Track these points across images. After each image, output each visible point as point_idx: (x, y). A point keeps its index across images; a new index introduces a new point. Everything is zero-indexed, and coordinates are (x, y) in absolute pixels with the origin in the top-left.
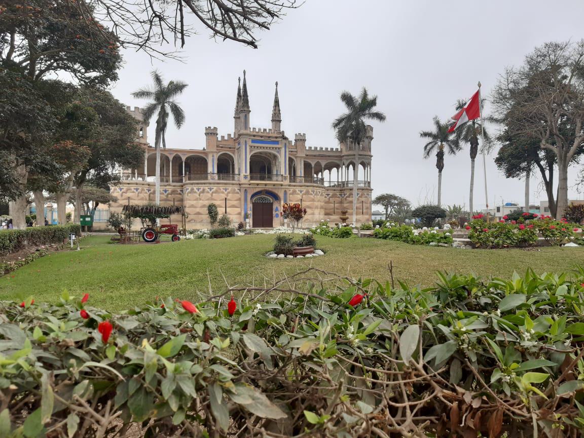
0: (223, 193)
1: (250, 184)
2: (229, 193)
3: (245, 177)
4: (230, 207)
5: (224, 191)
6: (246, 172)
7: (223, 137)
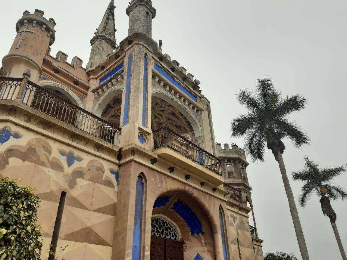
0: (57, 166)
1: (154, 161)
2: (79, 174)
3: (143, 134)
4: (72, 237)
5: (63, 160)
6: (145, 123)
7: (62, 56)
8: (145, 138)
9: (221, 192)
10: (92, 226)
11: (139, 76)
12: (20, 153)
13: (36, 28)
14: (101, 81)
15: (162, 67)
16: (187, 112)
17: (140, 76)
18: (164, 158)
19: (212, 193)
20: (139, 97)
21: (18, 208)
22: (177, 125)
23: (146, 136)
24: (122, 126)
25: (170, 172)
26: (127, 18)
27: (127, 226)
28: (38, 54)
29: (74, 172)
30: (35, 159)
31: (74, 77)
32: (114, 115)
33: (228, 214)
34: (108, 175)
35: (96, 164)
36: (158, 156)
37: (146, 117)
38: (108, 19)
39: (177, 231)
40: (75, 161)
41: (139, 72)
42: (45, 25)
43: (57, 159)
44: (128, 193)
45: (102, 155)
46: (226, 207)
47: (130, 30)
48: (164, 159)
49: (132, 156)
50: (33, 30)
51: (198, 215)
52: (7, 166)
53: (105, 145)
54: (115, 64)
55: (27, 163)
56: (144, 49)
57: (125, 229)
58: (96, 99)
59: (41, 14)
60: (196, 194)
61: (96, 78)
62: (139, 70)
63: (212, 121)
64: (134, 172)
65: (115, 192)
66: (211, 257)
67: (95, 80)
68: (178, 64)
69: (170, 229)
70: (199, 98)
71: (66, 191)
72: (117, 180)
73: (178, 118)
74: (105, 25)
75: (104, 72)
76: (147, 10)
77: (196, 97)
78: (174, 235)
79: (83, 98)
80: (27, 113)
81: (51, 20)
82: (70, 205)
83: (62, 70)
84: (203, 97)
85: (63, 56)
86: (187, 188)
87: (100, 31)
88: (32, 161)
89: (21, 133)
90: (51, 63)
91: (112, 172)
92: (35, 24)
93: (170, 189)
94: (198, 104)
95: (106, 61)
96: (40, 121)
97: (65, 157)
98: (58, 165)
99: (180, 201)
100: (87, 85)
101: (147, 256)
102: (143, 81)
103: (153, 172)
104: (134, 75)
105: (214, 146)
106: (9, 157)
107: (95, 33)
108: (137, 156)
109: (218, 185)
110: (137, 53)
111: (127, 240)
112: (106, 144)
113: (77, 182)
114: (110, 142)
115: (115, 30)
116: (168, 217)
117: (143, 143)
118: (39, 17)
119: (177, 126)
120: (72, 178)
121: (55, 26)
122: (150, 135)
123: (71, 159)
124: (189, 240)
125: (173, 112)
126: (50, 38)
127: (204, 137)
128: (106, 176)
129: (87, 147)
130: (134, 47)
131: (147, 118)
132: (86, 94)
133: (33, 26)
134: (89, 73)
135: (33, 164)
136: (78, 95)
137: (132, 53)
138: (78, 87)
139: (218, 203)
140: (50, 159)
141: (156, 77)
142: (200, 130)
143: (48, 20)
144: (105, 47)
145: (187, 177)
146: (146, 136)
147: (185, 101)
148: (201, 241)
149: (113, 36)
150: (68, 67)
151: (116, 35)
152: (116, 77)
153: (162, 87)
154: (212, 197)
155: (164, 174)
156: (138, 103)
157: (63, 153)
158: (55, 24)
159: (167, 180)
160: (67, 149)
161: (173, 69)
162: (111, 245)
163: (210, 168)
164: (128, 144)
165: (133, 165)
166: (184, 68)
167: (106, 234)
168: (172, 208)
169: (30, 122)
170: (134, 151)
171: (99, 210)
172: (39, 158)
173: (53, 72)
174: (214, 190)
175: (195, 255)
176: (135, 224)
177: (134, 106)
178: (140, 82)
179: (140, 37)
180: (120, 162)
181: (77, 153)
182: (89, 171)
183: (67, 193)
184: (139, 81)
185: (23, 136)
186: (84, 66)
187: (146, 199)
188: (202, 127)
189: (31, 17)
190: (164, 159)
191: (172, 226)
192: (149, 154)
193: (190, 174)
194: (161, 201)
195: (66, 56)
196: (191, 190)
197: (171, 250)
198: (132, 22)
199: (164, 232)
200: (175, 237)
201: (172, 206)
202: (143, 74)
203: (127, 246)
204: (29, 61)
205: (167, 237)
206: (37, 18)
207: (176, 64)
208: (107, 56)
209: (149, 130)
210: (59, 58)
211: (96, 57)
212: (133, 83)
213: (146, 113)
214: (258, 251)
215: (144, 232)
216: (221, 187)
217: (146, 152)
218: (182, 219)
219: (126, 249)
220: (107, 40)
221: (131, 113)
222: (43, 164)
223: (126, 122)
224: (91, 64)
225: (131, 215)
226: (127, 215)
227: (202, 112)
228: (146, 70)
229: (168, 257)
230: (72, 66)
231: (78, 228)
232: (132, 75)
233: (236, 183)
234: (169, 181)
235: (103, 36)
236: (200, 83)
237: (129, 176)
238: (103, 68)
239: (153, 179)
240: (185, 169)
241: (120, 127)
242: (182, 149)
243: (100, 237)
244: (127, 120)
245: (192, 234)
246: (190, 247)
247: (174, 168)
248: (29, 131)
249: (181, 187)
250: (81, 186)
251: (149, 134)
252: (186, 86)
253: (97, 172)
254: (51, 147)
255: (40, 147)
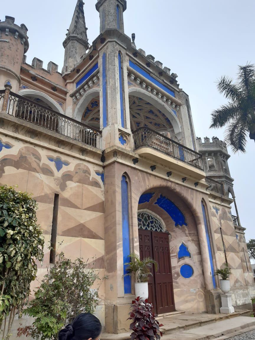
0: (47, 171)
1: (135, 161)
2: (68, 177)
3: (123, 135)
4: (68, 233)
5: (52, 166)
6: (124, 124)
7: (38, 62)
8: (126, 139)
9: (203, 186)
10: (85, 223)
11: (115, 75)
12: (14, 162)
13: (9, 37)
14: (77, 84)
15: (137, 63)
16: (165, 108)
17: (116, 75)
18: (146, 157)
19: (194, 187)
20: (116, 97)
21: (19, 211)
22: (155, 123)
23: (126, 137)
24: (103, 129)
25: (152, 170)
26: (98, 14)
27: (116, 221)
28: (15, 63)
29: (63, 176)
30: (28, 166)
31: (52, 83)
32: (93, 118)
33: (211, 206)
34: (94, 176)
35: (82, 167)
36: (140, 155)
37: (125, 118)
38: (78, 17)
39: (162, 223)
40: (63, 165)
41: (115, 72)
42: (18, 32)
43: (47, 165)
44: (114, 192)
45: (87, 158)
46: (208, 199)
47: (102, 27)
48: (145, 158)
49: (114, 158)
50: (7, 39)
51: (181, 208)
52: (3, 174)
53: (89, 149)
54: (90, 65)
55: (20, 170)
56: (118, 46)
57: (114, 224)
58: (75, 103)
59: (12, 21)
60: (178, 189)
61: (73, 82)
62: (114, 69)
63: (191, 116)
64: (118, 173)
65: (102, 191)
66: (196, 246)
67: (72, 84)
68: (153, 58)
69: (155, 222)
70: (178, 93)
71: (58, 193)
72: (103, 181)
73: (156, 115)
74: (76, 24)
75: (80, 75)
76: (117, 3)
77: (174, 92)
78: (159, 227)
79: (62, 103)
80: (14, 123)
81: (23, 26)
82: (64, 205)
83: (39, 77)
84: (181, 91)
85: (38, 62)
86: (169, 184)
87: (71, 31)
88: (25, 168)
89: (11, 143)
90: (28, 71)
91: (98, 173)
92: (7, 32)
93: (153, 186)
94: (177, 99)
95: (81, 63)
96: (27, 131)
97: (54, 162)
98: (48, 170)
99: (163, 196)
100: (65, 90)
101: (136, 246)
102: (118, 81)
103: (135, 171)
104: (109, 75)
105: (194, 141)
106: (5, 166)
107: (67, 35)
108: (119, 157)
109: (200, 180)
110: (111, 51)
111: (117, 233)
112: (89, 148)
113: (67, 185)
114: (93, 146)
115: (86, 29)
116: (153, 211)
117: (123, 144)
118: (11, 24)
119: (156, 124)
120: (62, 181)
121: (28, 32)
122: (130, 136)
123: (59, 164)
124: (174, 231)
125: (151, 110)
126: (24, 45)
127: (184, 133)
128: (93, 178)
129: (72, 152)
130: (107, 45)
131: (126, 118)
132: (65, 100)
133: (7, 35)
134: (65, 78)
135: (26, 171)
136: (57, 101)
137: (106, 52)
138: (56, 93)
139: (200, 197)
140: (41, 165)
141: (132, 75)
142: (180, 126)
143: (20, 26)
144: (78, 48)
145: (169, 174)
146: (126, 137)
147: (162, 97)
148: (185, 232)
149: (85, 36)
150: (45, 74)
151: (87, 33)
152: (91, 79)
153: (138, 85)
154: (194, 191)
155: (147, 173)
156: (116, 105)
157: (51, 159)
158: (27, 30)
159: (149, 177)
160: (55, 155)
161: (148, 64)
162: (103, 238)
163: (191, 163)
164: (110, 146)
165: (116, 165)
166: (160, 62)
167: (98, 229)
168: (156, 203)
169: (18, 132)
170: (116, 153)
171: (88, 209)
172: (31, 165)
173: (31, 81)
174: (196, 184)
175: (180, 244)
176: (123, 218)
177: (112, 108)
178: (116, 82)
179: (112, 33)
180: (104, 164)
181: (64, 158)
182: (77, 174)
183: (59, 195)
184: (115, 81)
185: (14, 146)
186: (60, 70)
187: (131, 196)
188: (181, 122)
189: (3, 25)
190: (145, 158)
191: (157, 219)
192: (131, 154)
193: (171, 170)
194: (145, 198)
195: (41, 62)
196: (173, 186)
197: (157, 241)
198: (103, 18)
199: (150, 225)
200: (160, 229)
201: (156, 201)
202: (118, 73)
203: (117, 238)
204: (8, 71)
205: (153, 229)
206: (9, 26)
207: (151, 58)
208: (81, 58)
209: (128, 130)
210: (35, 65)
211: (70, 60)
212: (109, 84)
213: (124, 114)
214: (241, 238)
215: (132, 226)
216: (203, 181)
217: (128, 153)
218: (166, 212)
219: (117, 241)
220: (79, 40)
221: (109, 115)
222: (35, 170)
223: (106, 124)
224: (66, 68)
225: (119, 211)
226: (115, 211)
227: (181, 107)
228: (121, 68)
229: (155, 247)
230: (48, 72)
231: (72, 225)
232: (108, 75)
233: (218, 175)
234: (152, 179)
235: (75, 37)
236: (177, 77)
237: (114, 177)
238: (78, 71)
239: (136, 178)
240: (166, 166)
241: (100, 130)
242: (163, 147)
243: (93, 232)
244: (107, 122)
245: (176, 225)
246: (175, 237)
247: (155, 166)
248: (18, 140)
249: (164, 183)
250: (71, 188)
251: (129, 135)
252: (163, 81)
253: (84, 174)
254: (39, 154)
255: (30, 155)
